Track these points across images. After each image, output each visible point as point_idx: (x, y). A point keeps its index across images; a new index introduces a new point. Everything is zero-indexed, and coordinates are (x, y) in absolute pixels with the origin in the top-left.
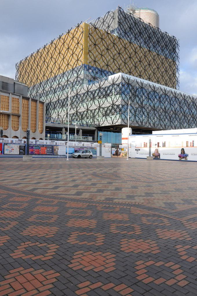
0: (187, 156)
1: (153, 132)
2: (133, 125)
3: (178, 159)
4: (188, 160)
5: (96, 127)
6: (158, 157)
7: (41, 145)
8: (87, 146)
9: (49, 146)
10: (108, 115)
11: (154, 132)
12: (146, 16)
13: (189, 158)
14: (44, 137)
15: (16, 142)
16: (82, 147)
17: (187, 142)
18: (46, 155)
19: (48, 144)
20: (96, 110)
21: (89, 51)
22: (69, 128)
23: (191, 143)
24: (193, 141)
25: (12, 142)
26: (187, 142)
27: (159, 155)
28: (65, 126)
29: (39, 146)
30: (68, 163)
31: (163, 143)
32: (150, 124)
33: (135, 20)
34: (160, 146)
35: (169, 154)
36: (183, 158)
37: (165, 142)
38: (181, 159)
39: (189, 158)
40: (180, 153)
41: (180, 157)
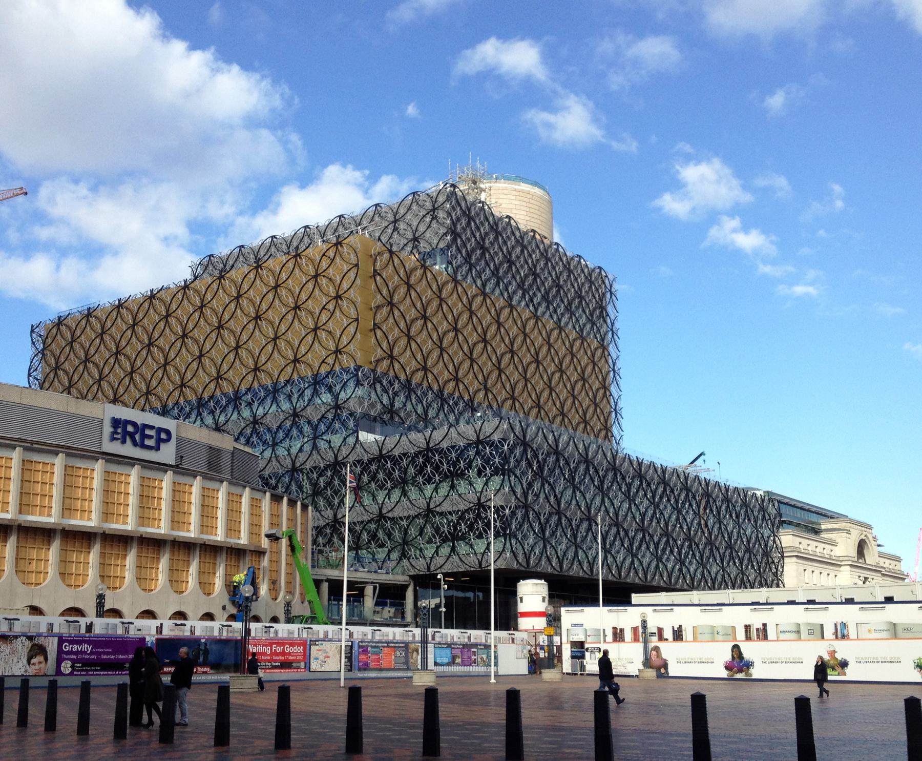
0: (749, 665)
1: (633, 595)
2: (539, 570)
3: (724, 674)
4: (754, 677)
5: (410, 576)
6: (663, 671)
7: (383, 643)
8: (478, 641)
9: (400, 643)
10: (463, 538)
11: (636, 598)
12: (517, 202)
13: (757, 672)
14: (321, 614)
15: (335, 637)
16: (467, 644)
17: (747, 628)
18: (395, 670)
19: (398, 638)
20: (413, 518)
21: (375, 324)
22: (348, 582)
23: (758, 630)
24: (765, 625)
25: (326, 639)
26: (746, 626)
27: (665, 665)
28: (333, 573)
29: (380, 645)
30: (492, 688)
31: (676, 629)
32: (549, 560)
33: (495, 222)
34: (667, 640)
35: (695, 662)
36: (740, 671)
37: (681, 626)
38: (733, 675)
39: (757, 672)
40: (728, 657)
41: (728, 667)
